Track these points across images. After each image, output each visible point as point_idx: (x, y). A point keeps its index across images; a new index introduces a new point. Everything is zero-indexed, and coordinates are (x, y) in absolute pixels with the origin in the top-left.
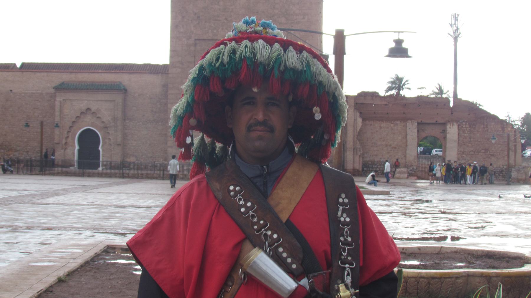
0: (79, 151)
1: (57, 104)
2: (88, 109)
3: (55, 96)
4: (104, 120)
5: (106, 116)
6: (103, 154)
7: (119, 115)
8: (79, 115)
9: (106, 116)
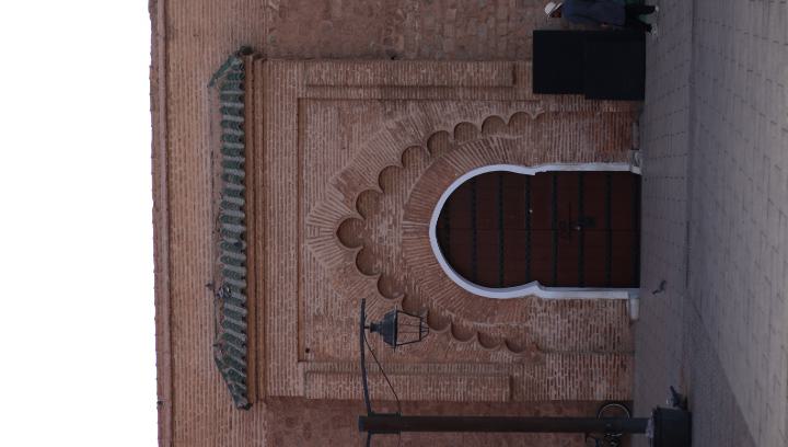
0: (545, 284)
1: (319, 389)
2: (343, 232)
3: (287, 401)
4: (392, 153)
5: (378, 140)
6: (563, 161)
7: (366, 73)
8: (374, 281)
9: (378, 140)
